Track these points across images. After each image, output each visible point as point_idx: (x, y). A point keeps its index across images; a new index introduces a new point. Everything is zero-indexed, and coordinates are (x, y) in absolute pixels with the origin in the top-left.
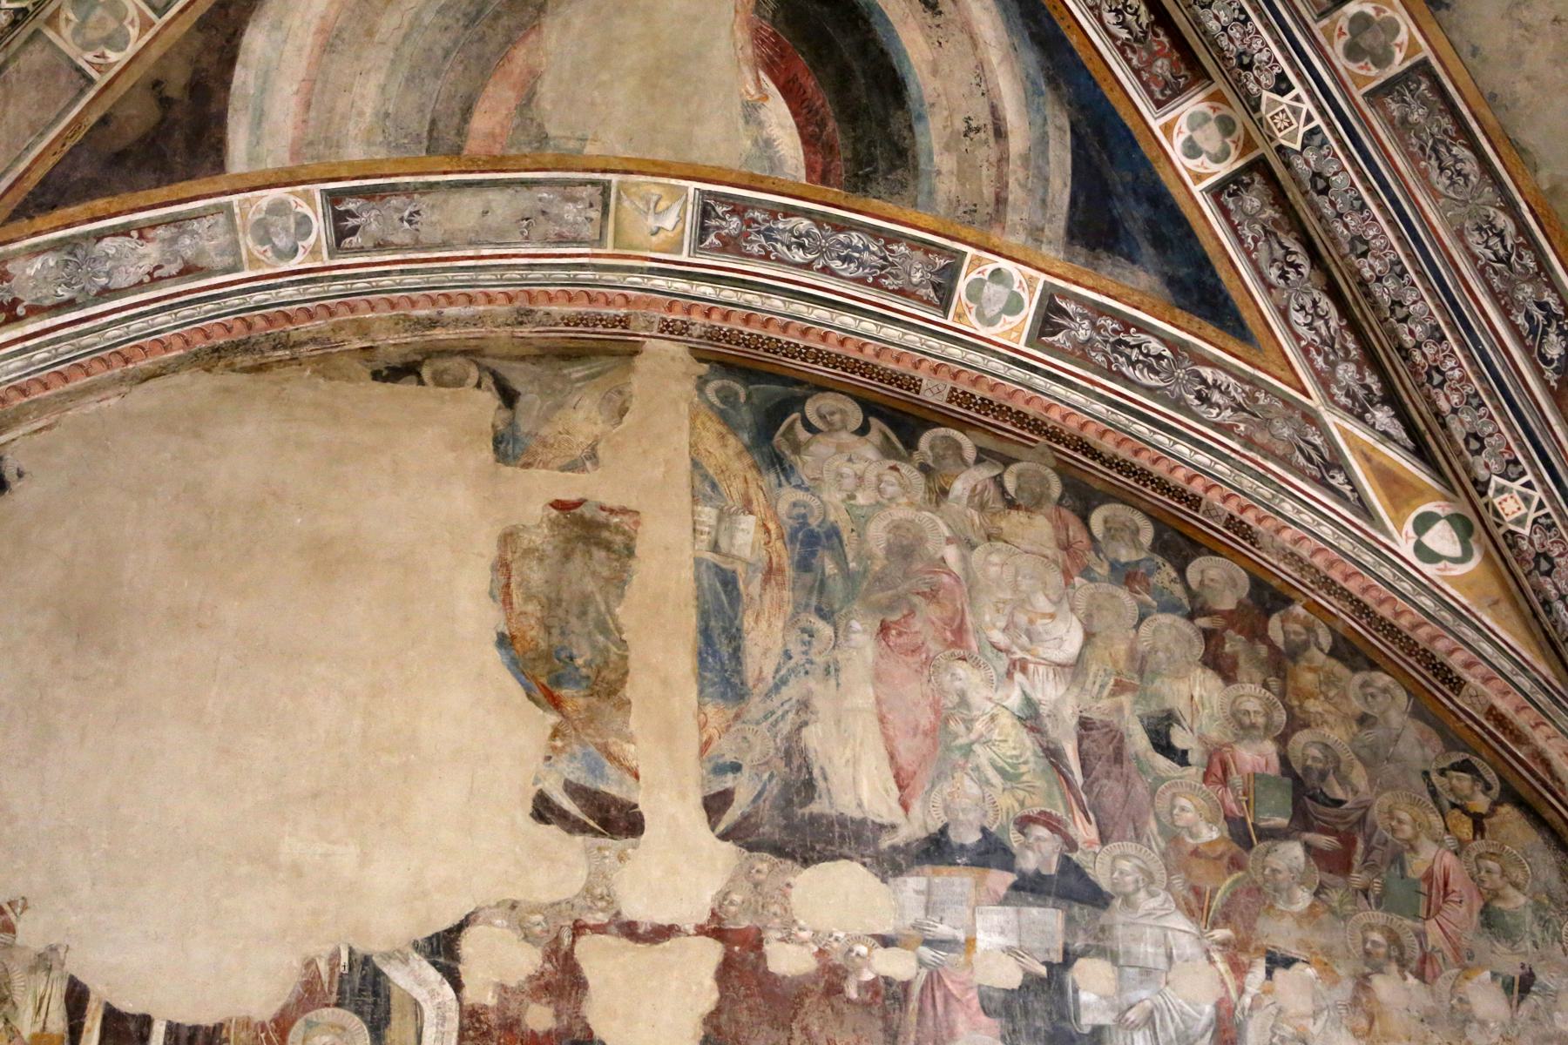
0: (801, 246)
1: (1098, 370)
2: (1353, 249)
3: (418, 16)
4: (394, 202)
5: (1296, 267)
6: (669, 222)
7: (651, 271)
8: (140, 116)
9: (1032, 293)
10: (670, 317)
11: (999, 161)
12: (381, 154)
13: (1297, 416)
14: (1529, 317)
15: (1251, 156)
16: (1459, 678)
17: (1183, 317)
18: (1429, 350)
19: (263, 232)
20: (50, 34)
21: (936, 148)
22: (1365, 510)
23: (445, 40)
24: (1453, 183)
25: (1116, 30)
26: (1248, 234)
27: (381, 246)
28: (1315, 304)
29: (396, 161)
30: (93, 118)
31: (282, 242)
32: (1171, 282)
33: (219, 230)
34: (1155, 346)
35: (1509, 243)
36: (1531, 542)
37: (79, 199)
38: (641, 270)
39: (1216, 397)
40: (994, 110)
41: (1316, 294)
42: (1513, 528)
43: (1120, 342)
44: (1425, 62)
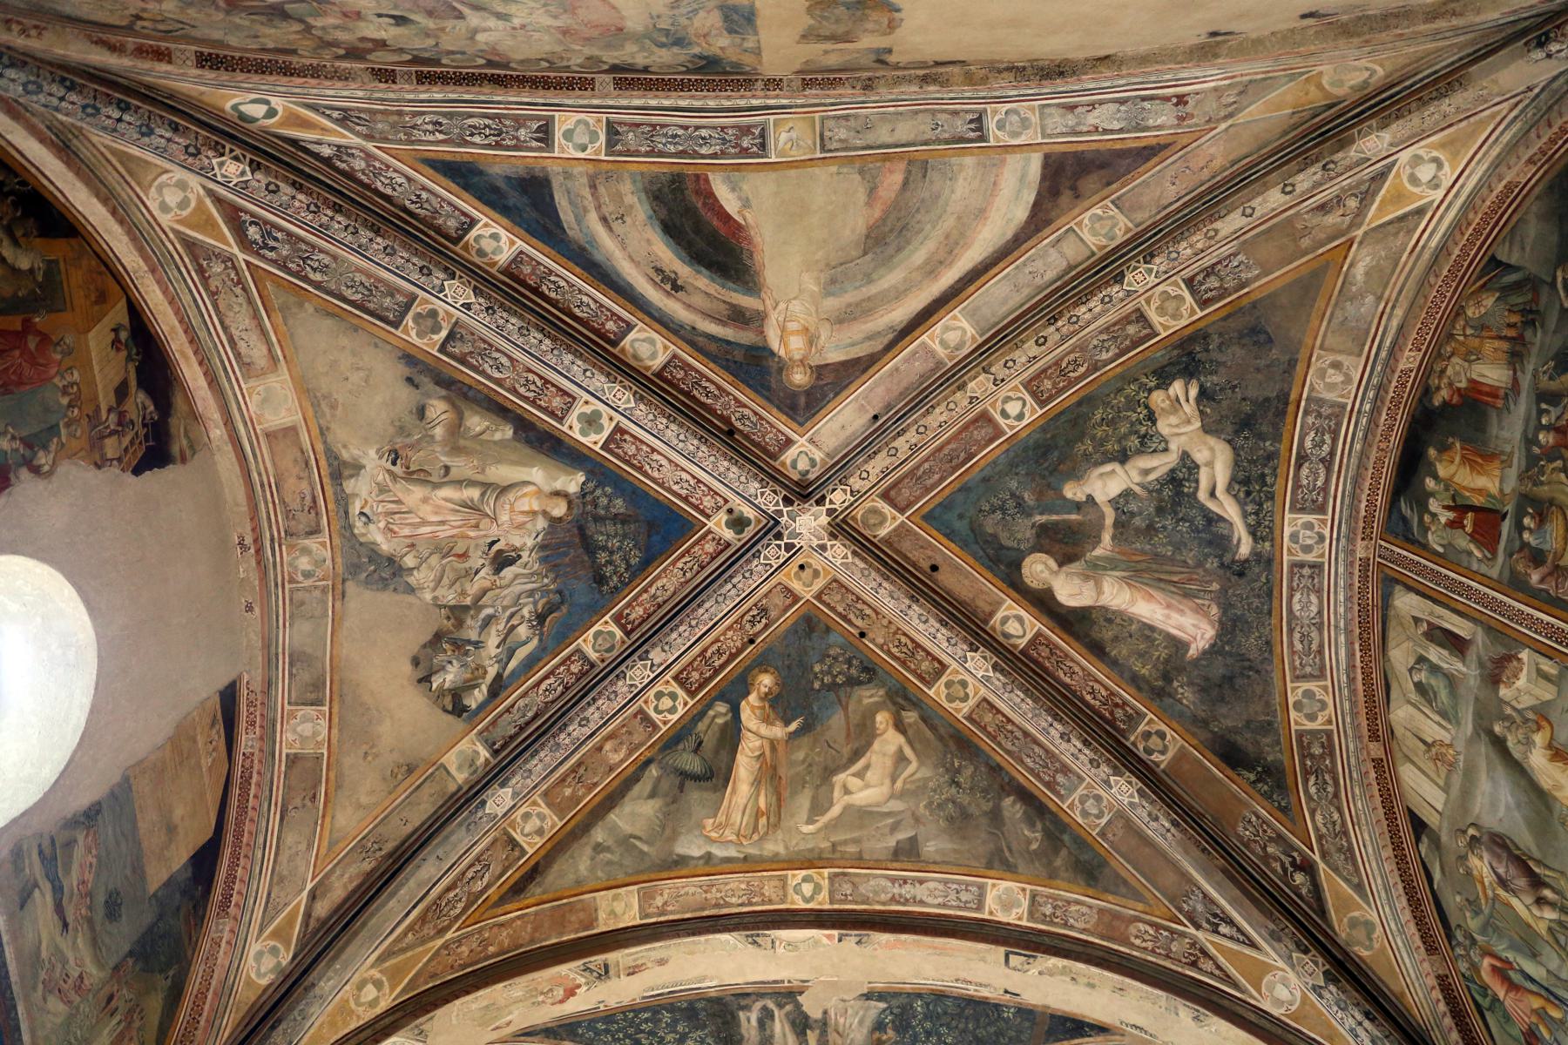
0: (703, 138)
1: (506, 116)
2: (393, 248)
3: (934, 227)
4: (947, 135)
5: (413, 202)
6: (784, 137)
7: (791, 107)
8: (1089, 183)
9: (560, 144)
10: (778, 92)
11: (600, 207)
12: (954, 160)
13: (377, 136)
14: (276, 239)
15: (462, 244)
16: (203, 67)
17: (466, 158)
18: (325, 219)
19: (1025, 124)
20: (1130, 225)
21: (638, 205)
22: (314, 108)
23: (918, 217)
24: (353, 280)
25: (556, 279)
26: (446, 207)
27: (955, 113)
28: (394, 189)
29: (945, 156)
30: (1114, 186)
31: (1015, 118)
32: (481, 173)
33: (1051, 126)
34: (477, 139)
35: (308, 268)
36: (207, 157)
37: (1130, 150)
38: (797, 106)
39: (430, 127)
40: (610, 229)
41: (395, 194)
42: (223, 158)
43: (498, 135)
44: (397, 328)
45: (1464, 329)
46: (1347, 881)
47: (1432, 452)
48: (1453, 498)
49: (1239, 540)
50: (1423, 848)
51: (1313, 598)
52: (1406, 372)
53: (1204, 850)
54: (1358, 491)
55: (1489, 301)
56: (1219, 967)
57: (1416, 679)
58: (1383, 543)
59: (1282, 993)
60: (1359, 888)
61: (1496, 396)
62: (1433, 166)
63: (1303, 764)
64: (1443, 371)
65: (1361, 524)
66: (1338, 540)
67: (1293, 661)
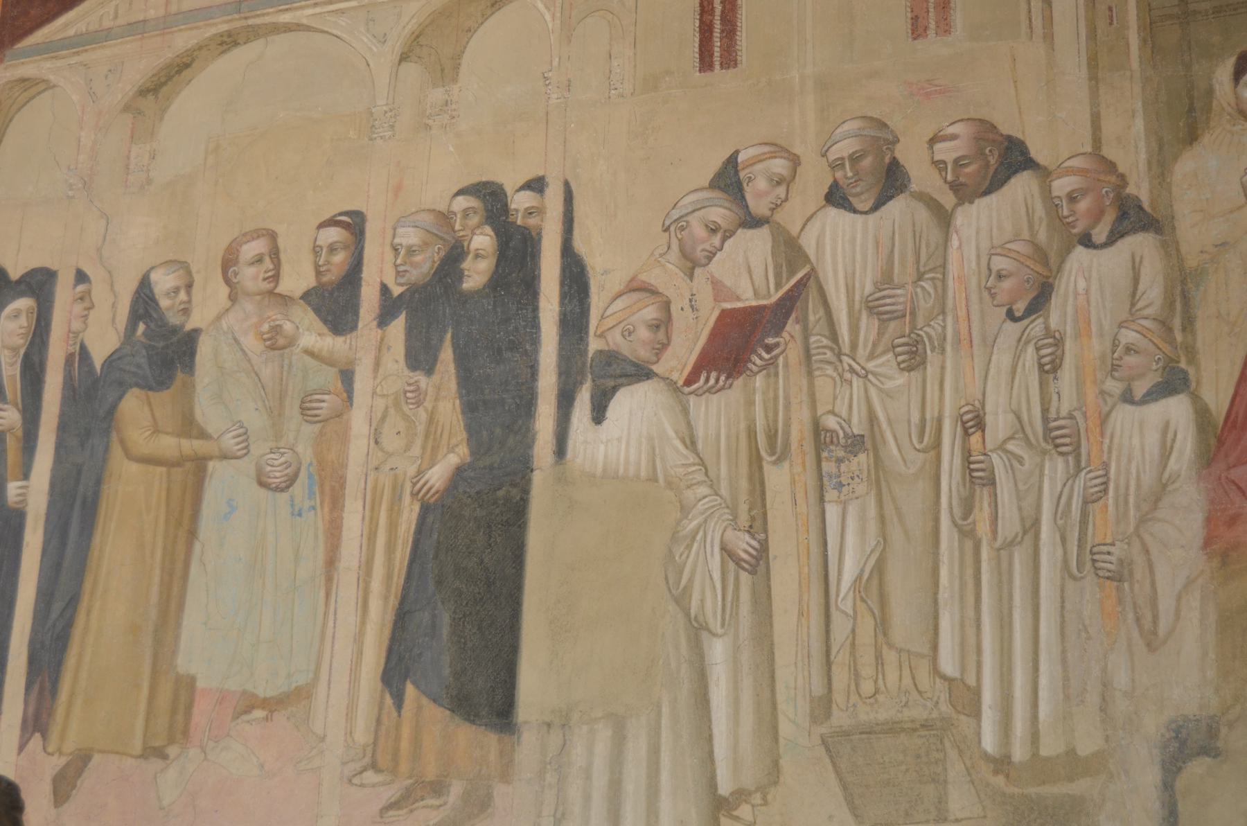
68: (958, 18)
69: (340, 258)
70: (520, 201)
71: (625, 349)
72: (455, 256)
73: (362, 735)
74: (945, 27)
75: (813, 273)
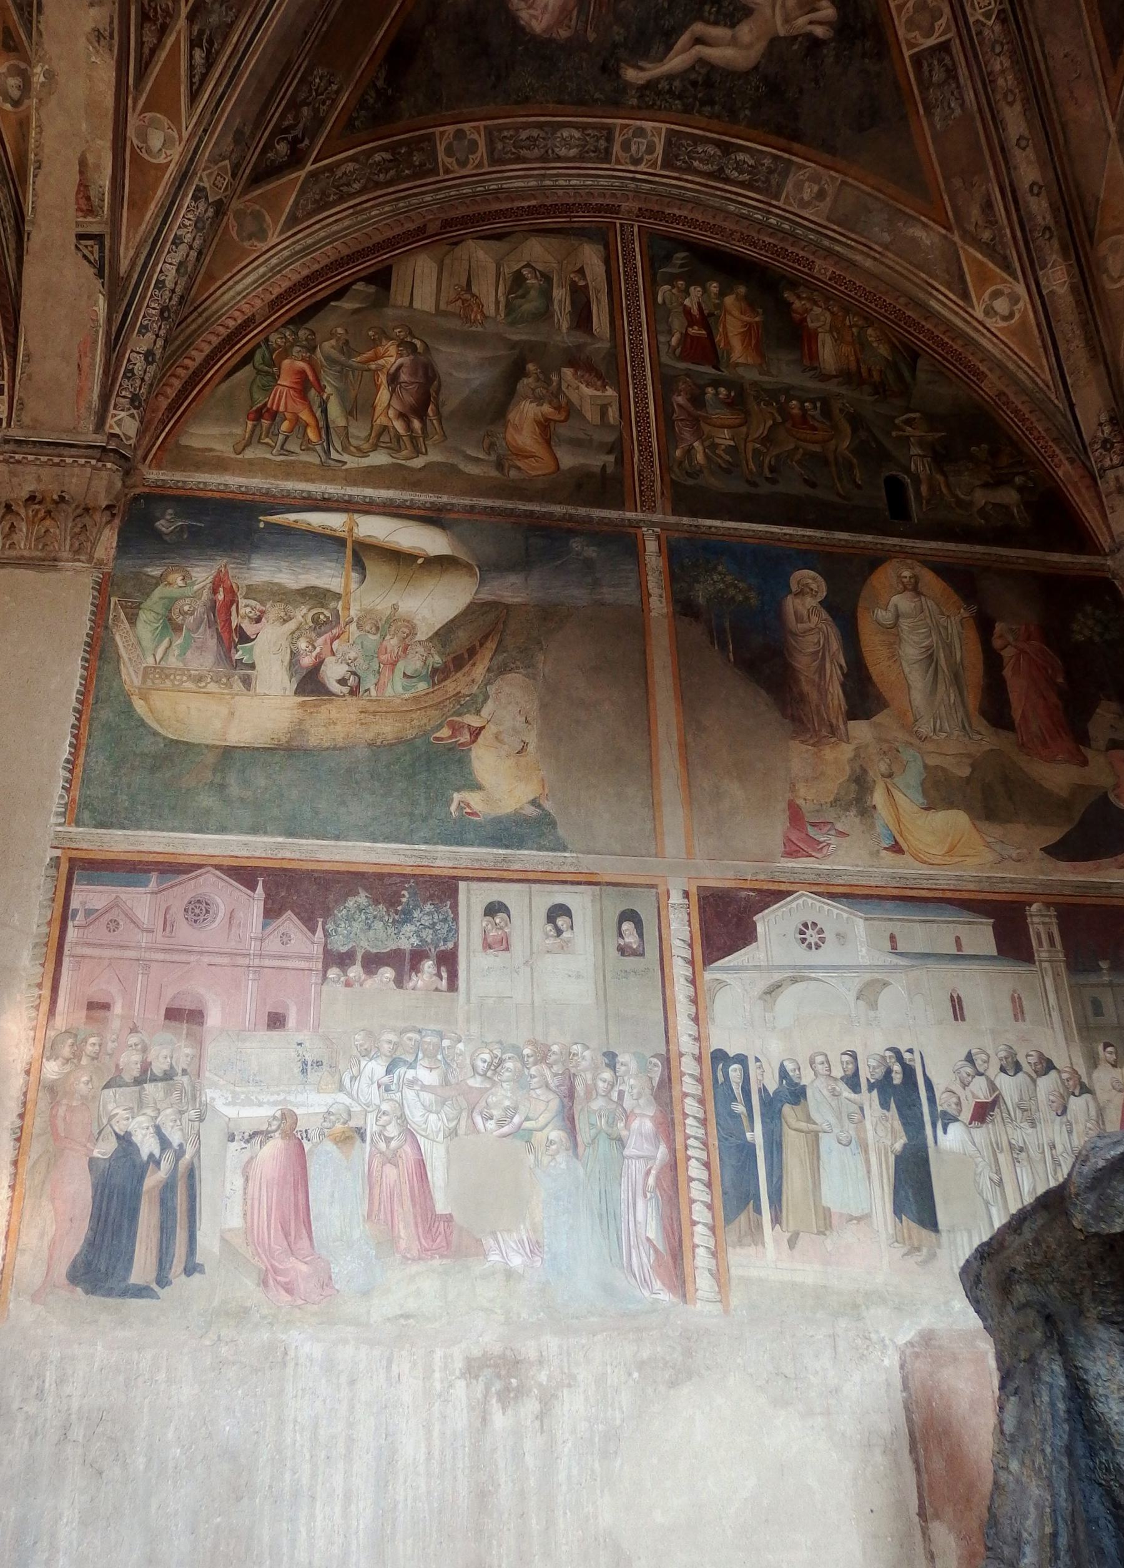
45: (857, 326)
46: (296, 202)
47: (742, 290)
48: (711, 315)
49: (642, 69)
50: (359, 286)
51: (573, 152)
52: (811, 265)
53: (306, 33)
54: (690, 206)
55: (883, 350)
56: (153, 51)
57: (525, 272)
58: (636, 229)
59: (156, 140)
60: (293, 220)
61: (811, 359)
62: (1006, 313)
63: (400, 143)
64: (815, 303)
65: (656, 208)
66: (633, 179)
67: (508, 129)
68: (1027, 1016)
69: (850, 1066)
70: (907, 1056)
71: (949, 1111)
72: (889, 1072)
73: (891, 1231)
74: (1024, 1020)
75: (1000, 1094)
